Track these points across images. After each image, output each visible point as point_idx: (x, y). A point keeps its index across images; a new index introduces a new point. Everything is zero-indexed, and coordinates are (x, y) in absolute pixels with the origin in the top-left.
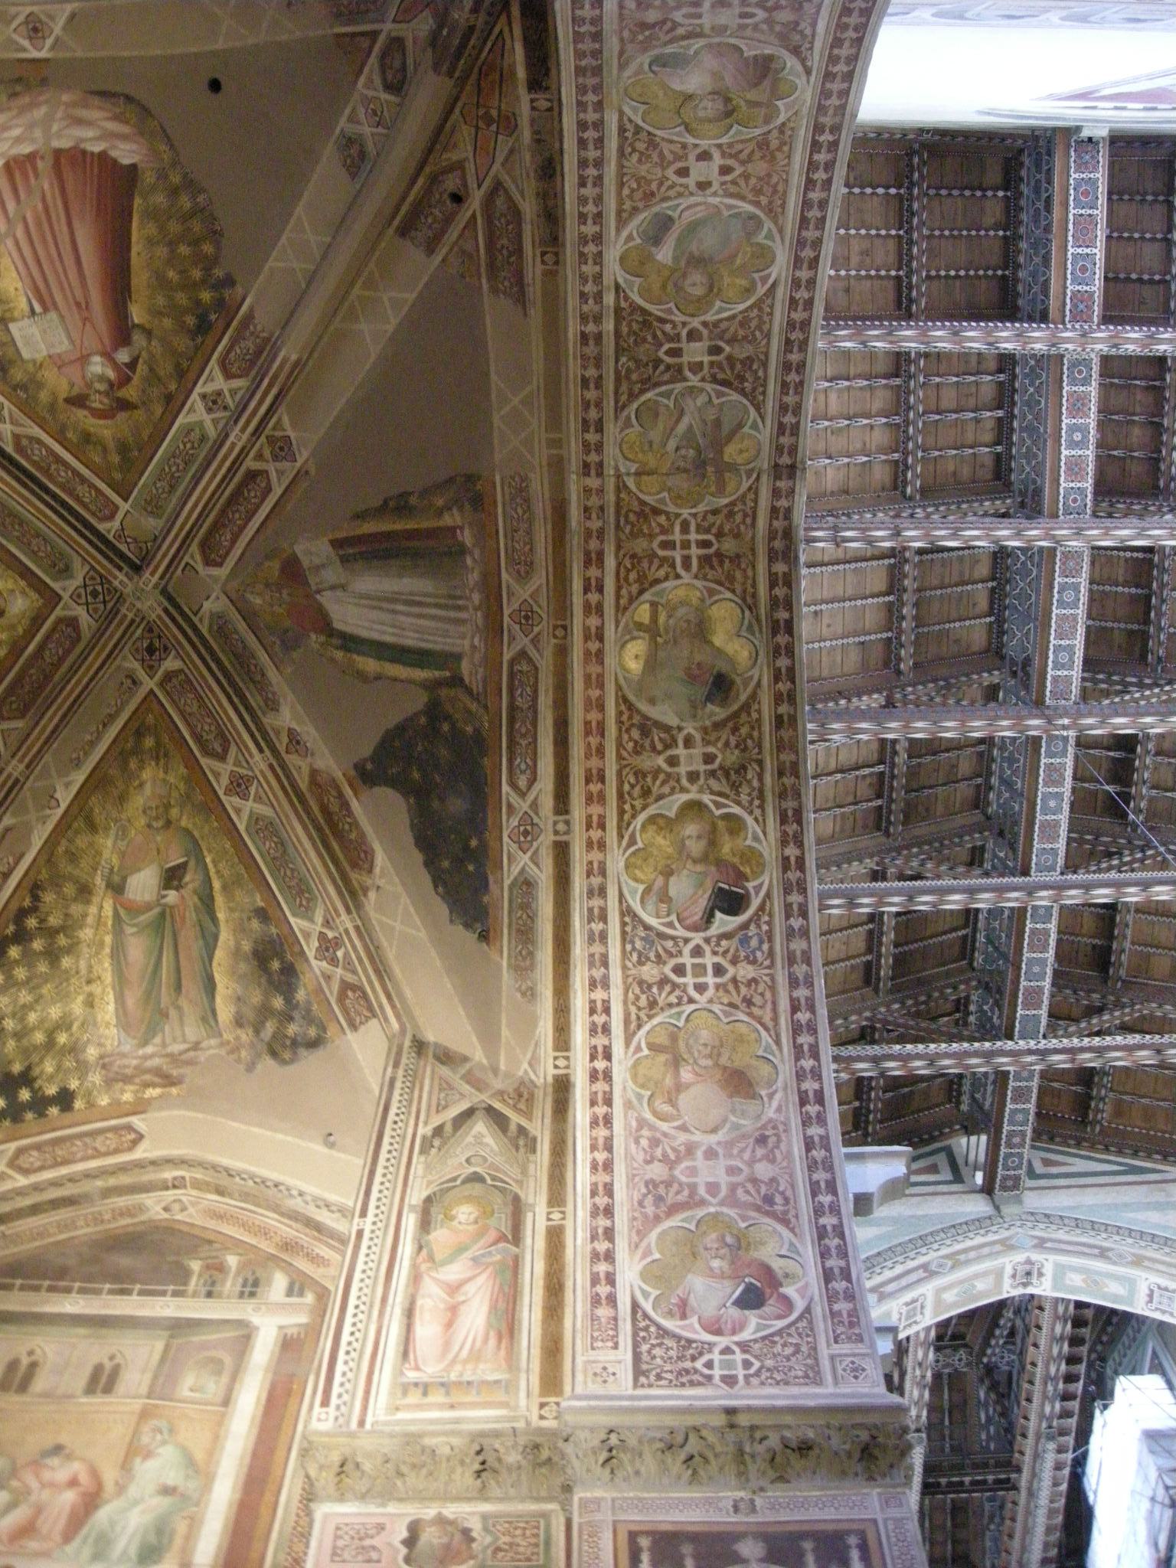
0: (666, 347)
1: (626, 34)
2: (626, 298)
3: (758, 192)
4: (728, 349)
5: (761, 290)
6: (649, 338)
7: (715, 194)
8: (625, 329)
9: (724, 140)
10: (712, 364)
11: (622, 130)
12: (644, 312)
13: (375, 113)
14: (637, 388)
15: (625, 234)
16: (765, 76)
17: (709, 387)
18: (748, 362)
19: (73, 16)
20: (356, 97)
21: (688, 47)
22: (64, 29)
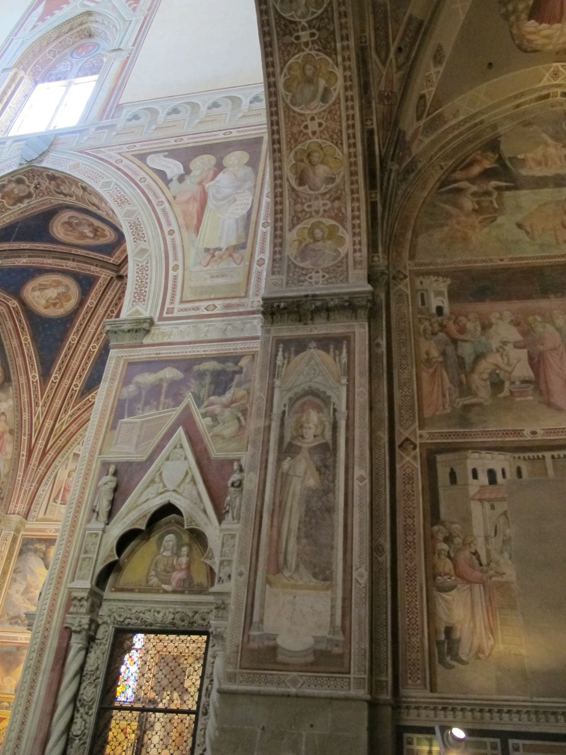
0: (316, 38)
1: (344, 193)
2: (333, 60)
3: (294, 117)
4: (293, 40)
5: (285, 70)
6: (323, 41)
7: (308, 115)
8: (333, 44)
9: (309, 141)
10: (298, 31)
11: (342, 144)
12: (326, 54)
13: (429, 81)
14: (325, 16)
15: (337, 92)
16: (301, 175)
17: (297, 20)
18: (285, 34)
19: (539, 82)
20: (436, 85)
21: (326, 188)
22: (544, 75)
